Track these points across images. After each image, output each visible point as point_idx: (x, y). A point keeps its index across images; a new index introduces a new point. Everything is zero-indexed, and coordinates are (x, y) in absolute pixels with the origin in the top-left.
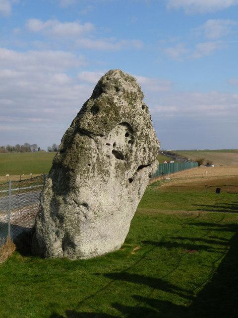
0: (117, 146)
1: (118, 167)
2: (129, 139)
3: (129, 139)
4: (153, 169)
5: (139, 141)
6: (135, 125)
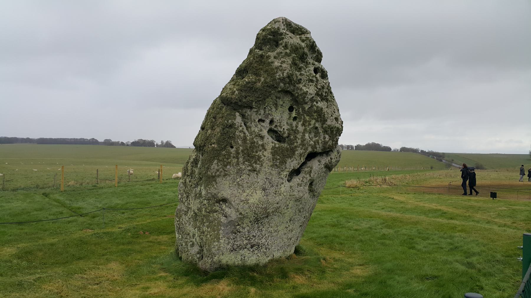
1: (275, 152)
2: (294, 114)
3: (294, 114)
4: (331, 159)
5: (307, 118)
6: (301, 95)
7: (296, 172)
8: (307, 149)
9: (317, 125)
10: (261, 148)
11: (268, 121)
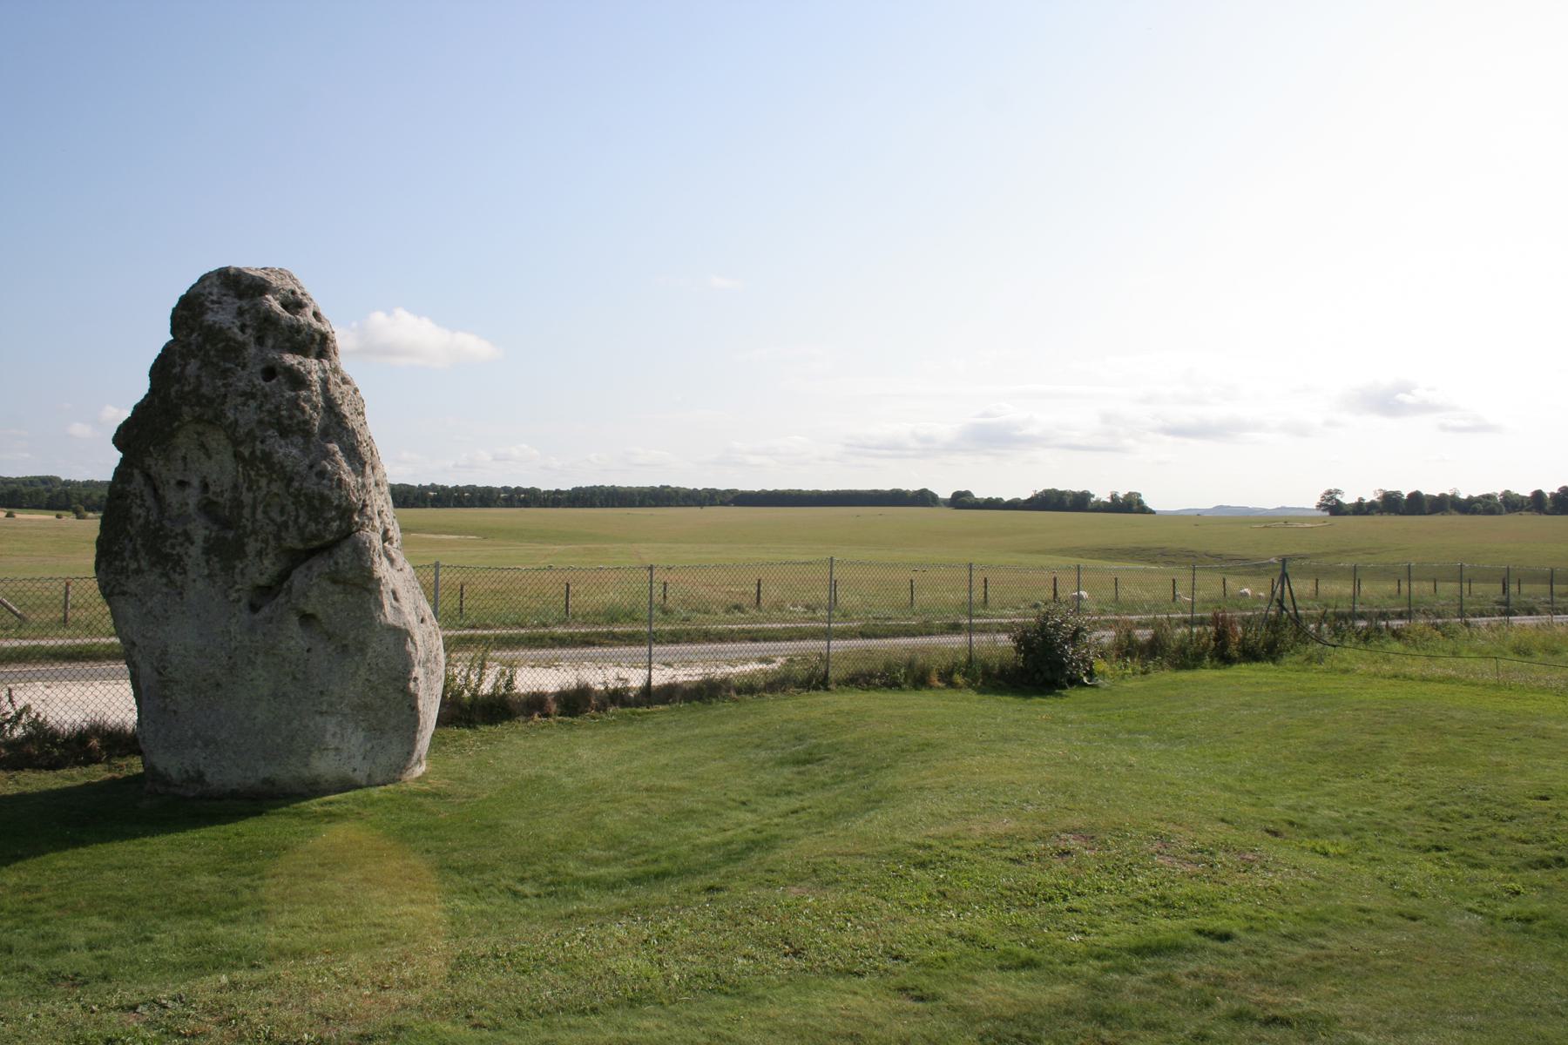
0: (212, 488)
7: (266, 593)
8: (266, 542)
9: (275, 488)
10: (181, 539)
11: (196, 482)
